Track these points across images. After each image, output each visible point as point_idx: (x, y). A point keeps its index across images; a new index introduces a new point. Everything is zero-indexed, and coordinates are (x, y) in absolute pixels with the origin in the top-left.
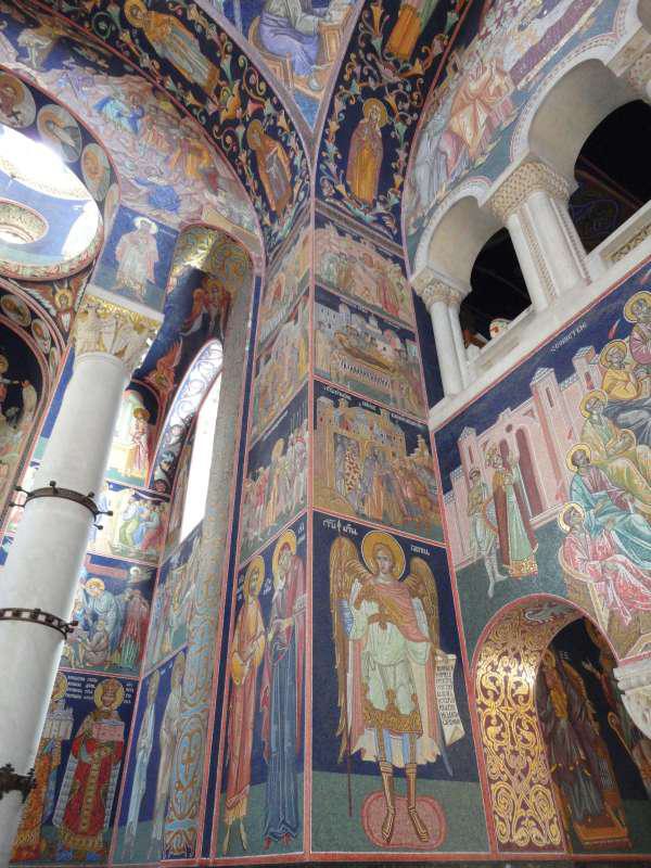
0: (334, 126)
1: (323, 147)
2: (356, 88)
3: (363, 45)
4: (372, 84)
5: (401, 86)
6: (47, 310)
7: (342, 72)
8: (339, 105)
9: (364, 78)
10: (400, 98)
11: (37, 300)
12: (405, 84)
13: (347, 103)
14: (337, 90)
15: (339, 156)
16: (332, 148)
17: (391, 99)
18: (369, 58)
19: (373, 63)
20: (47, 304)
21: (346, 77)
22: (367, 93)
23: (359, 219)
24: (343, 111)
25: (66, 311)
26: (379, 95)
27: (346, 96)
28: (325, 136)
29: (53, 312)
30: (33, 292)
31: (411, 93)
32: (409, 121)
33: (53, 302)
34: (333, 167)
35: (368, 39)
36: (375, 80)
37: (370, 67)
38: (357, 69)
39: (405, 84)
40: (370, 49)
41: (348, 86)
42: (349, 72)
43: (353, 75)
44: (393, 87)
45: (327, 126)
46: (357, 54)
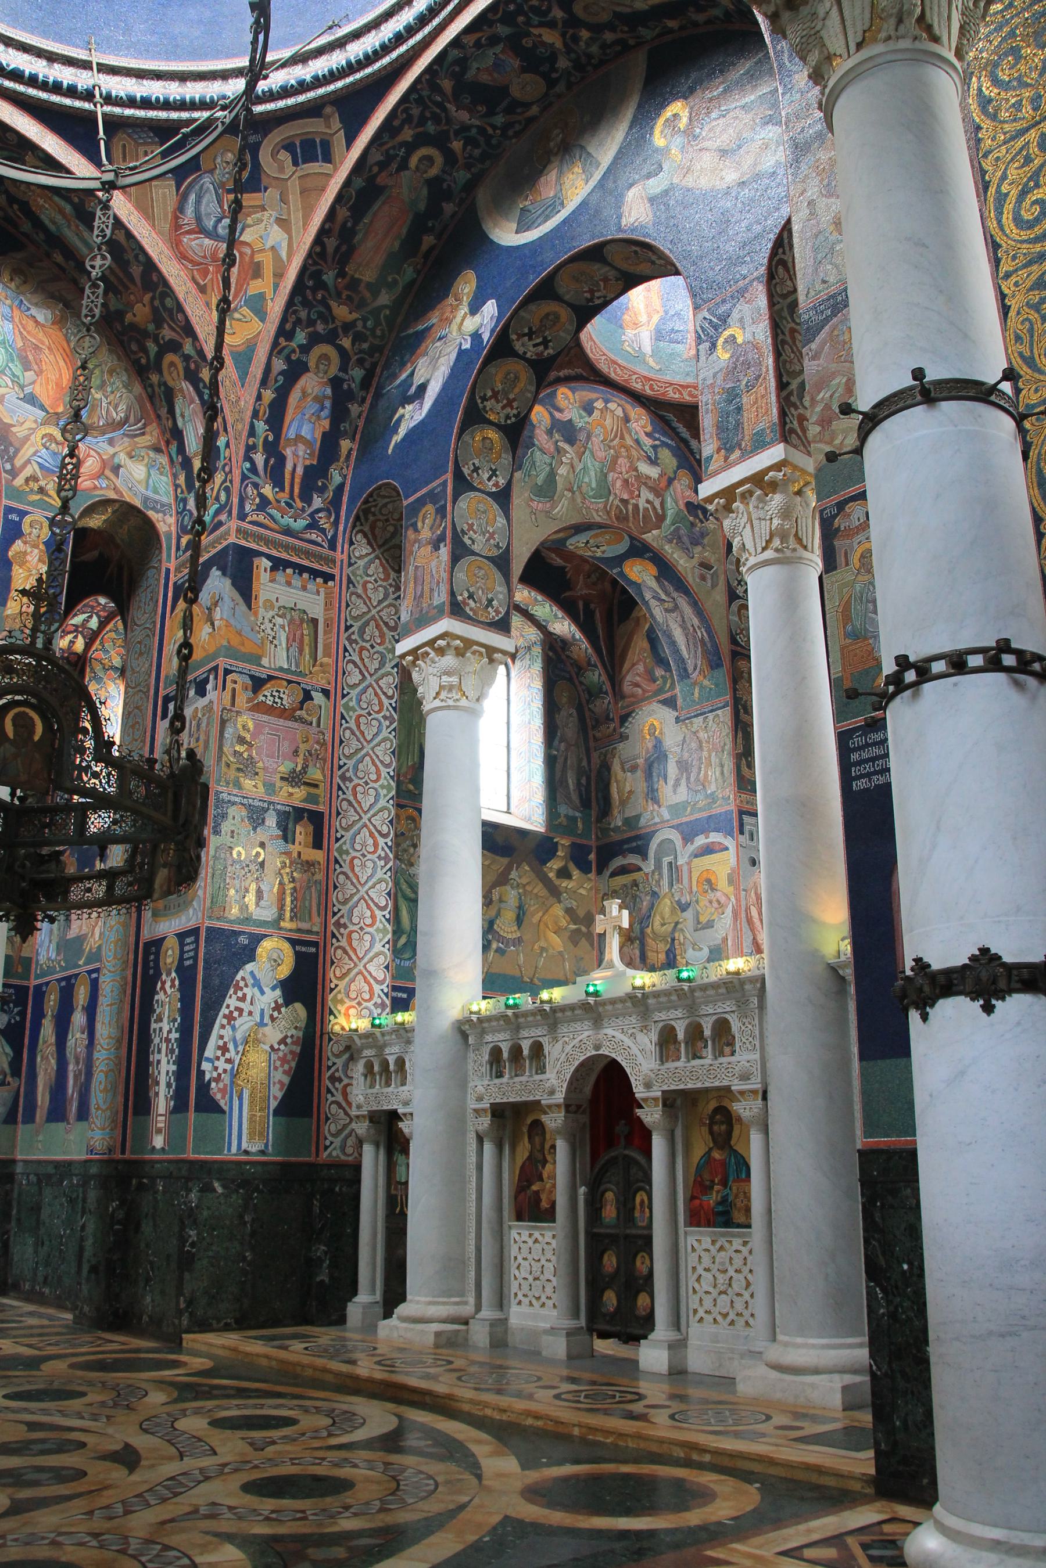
0: (268, 395)
1: (252, 432)
2: (301, 337)
3: (311, 283)
4: (320, 327)
5: (360, 324)
7: (284, 320)
8: (279, 365)
9: (311, 323)
10: (358, 338)
12: (365, 320)
13: (288, 359)
14: (275, 344)
15: (271, 438)
16: (261, 426)
17: (346, 343)
18: (319, 296)
19: (324, 302)
21: (288, 326)
22: (315, 339)
23: (288, 531)
24: (281, 373)
26: (331, 338)
27: (286, 351)
28: (255, 414)
31: (373, 331)
32: (367, 365)
34: (259, 458)
35: (317, 275)
36: (326, 322)
37: (321, 309)
38: (303, 314)
39: (365, 320)
40: (321, 285)
41: (290, 336)
42: (292, 319)
43: (298, 322)
44: (347, 327)
45: (259, 397)
46: (304, 297)
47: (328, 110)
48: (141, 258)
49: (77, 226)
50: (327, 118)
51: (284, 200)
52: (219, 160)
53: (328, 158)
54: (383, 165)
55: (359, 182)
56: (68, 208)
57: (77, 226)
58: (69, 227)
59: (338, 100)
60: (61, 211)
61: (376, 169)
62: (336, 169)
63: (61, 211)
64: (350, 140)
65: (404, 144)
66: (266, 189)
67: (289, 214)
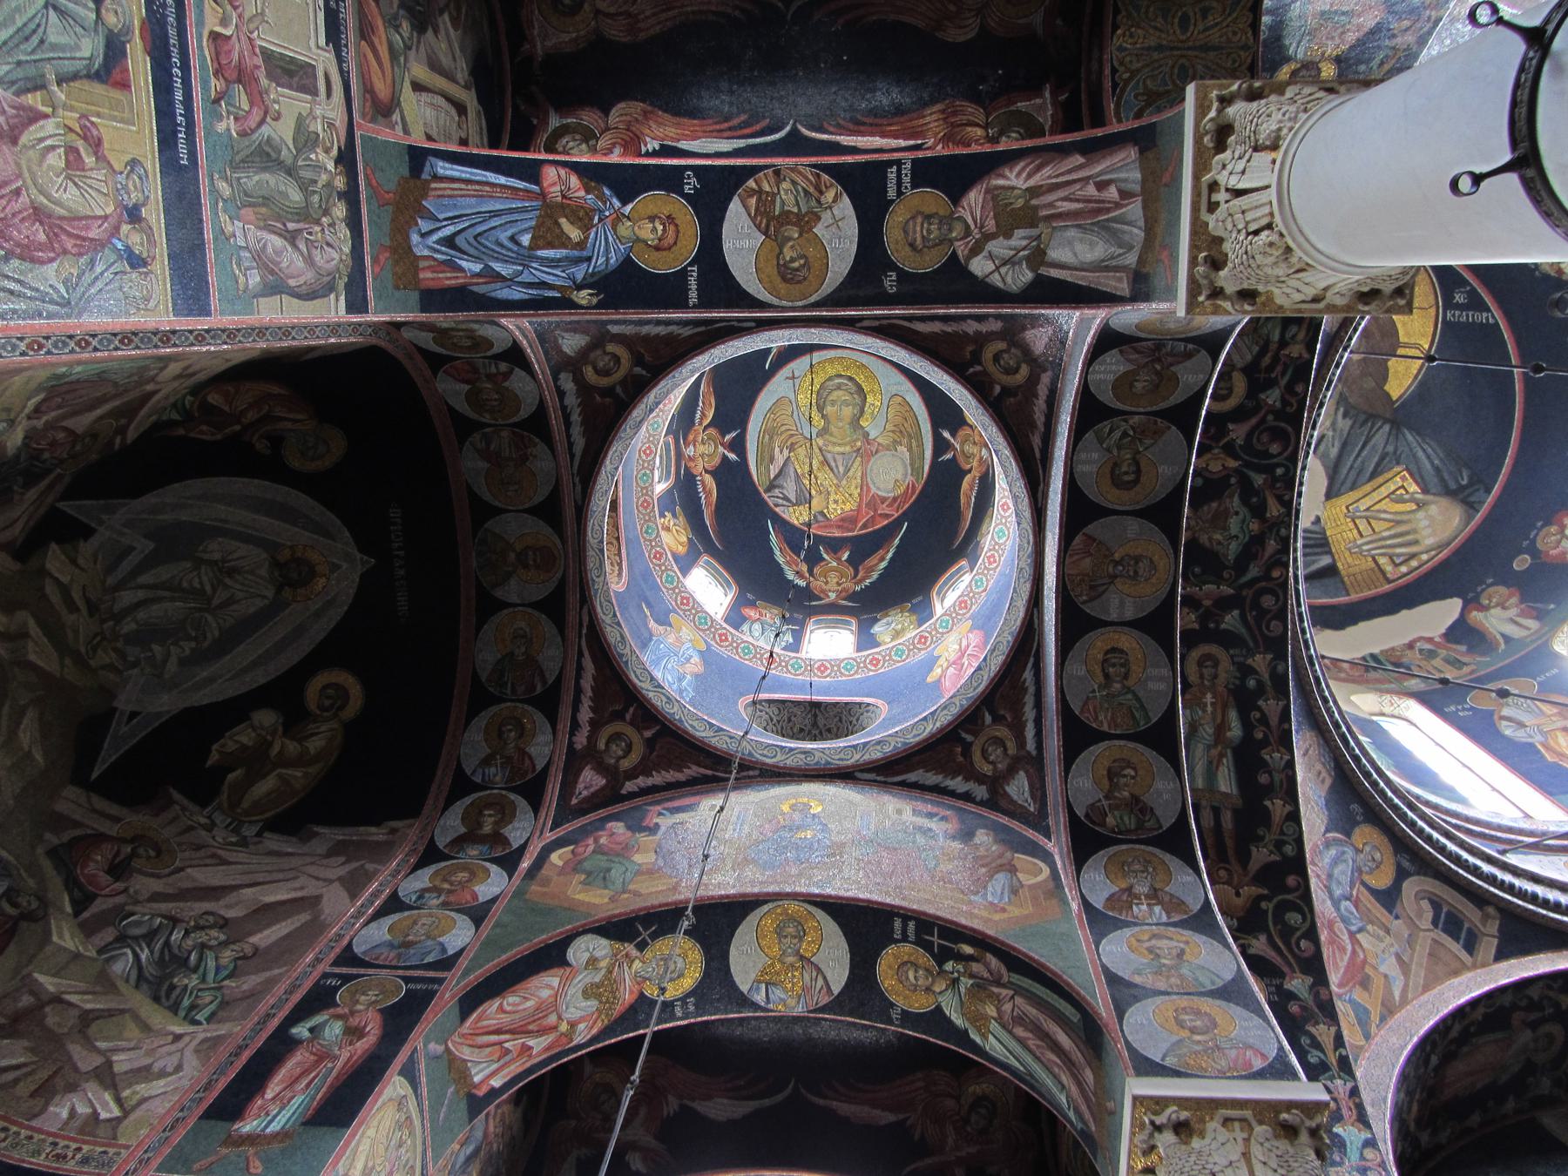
6: (575, 725)
11: (579, 691)
20: (585, 715)
25: (601, 768)
29: (581, 740)
30: (588, 663)
33: (595, 725)
47: (1491, 910)
48: (1289, 850)
49: (1221, 755)
50: (1486, 917)
51: (1411, 942)
52: (1367, 848)
53: (1470, 947)
54: (1533, 1006)
55: (1507, 1000)
56: (1235, 731)
57: (1221, 755)
58: (1209, 747)
59: (1506, 911)
60: (1221, 729)
61: (1524, 1003)
62: (1475, 967)
63: (1221, 729)
64: (1501, 955)
65: (1557, 1005)
66: (1397, 917)
67: (1411, 960)
